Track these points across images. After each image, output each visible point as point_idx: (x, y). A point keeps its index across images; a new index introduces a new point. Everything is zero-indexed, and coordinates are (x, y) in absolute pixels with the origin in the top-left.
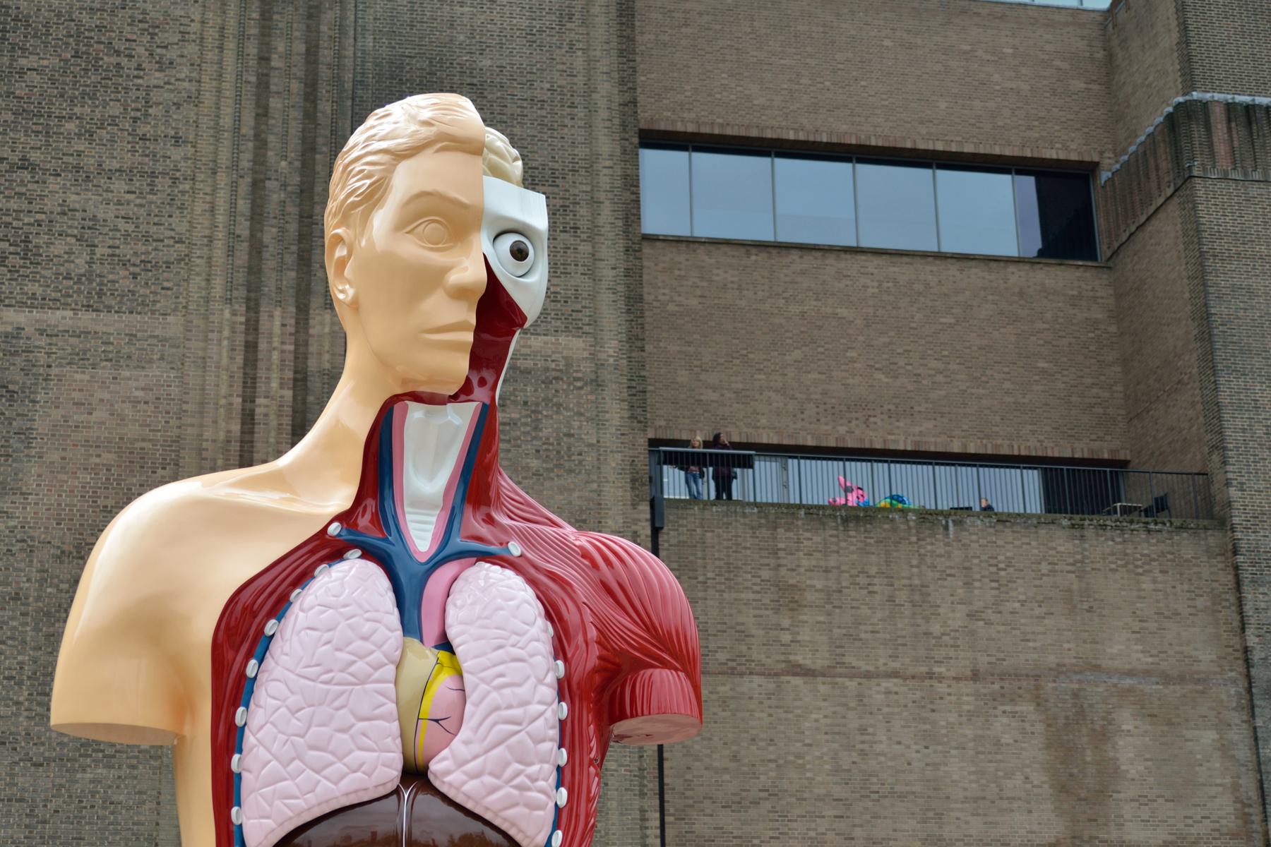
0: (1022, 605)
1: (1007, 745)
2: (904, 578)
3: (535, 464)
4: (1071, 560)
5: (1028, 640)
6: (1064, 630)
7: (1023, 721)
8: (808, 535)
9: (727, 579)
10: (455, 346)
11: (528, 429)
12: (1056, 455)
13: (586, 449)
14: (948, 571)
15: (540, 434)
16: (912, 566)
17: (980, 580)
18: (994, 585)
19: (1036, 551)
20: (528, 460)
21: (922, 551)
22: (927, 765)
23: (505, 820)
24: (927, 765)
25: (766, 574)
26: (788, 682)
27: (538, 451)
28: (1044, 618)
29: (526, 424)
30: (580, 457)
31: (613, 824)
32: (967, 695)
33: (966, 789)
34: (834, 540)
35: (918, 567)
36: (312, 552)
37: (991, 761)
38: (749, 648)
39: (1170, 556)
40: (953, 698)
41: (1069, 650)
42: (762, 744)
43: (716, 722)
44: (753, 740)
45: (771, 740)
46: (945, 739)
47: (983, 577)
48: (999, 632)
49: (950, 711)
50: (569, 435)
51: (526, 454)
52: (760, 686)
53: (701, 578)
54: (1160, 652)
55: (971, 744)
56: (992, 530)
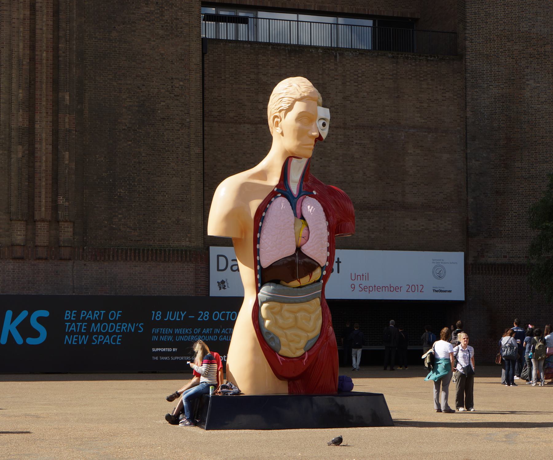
0: (368, 94)
1: (357, 158)
2: (315, 80)
3: (161, 32)
4: (391, 73)
5: (369, 111)
6: (386, 106)
7: (364, 148)
8: (273, 58)
9: (235, 78)
10: (310, 149)
11: (158, 15)
12: (386, 14)
13: (184, 26)
14: (336, 77)
15: (164, 18)
16: (319, 74)
17: (349, 82)
18: (356, 84)
19: (375, 69)
20: (158, 31)
21: (324, 67)
22: (321, 166)
23: (318, 260)
24: (321, 166)
25: (253, 76)
26: (261, 127)
27: (163, 26)
28: (377, 100)
29: (157, 13)
30: (181, 29)
31: (193, 195)
32: (341, 135)
33: (337, 178)
34: (284, 61)
35: (321, 75)
36: (271, 195)
37: (349, 166)
38: (244, 111)
39: (436, 73)
40: (334, 136)
41: (387, 115)
42: (248, 155)
43: (228, 145)
44: (244, 153)
45: (252, 154)
46: (330, 155)
47: (351, 80)
48: (356, 106)
49: (332, 142)
50: (177, 19)
51: (157, 28)
52: (248, 129)
53: (223, 78)
54: (428, 117)
55: (341, 158)
56: (356, 58)
